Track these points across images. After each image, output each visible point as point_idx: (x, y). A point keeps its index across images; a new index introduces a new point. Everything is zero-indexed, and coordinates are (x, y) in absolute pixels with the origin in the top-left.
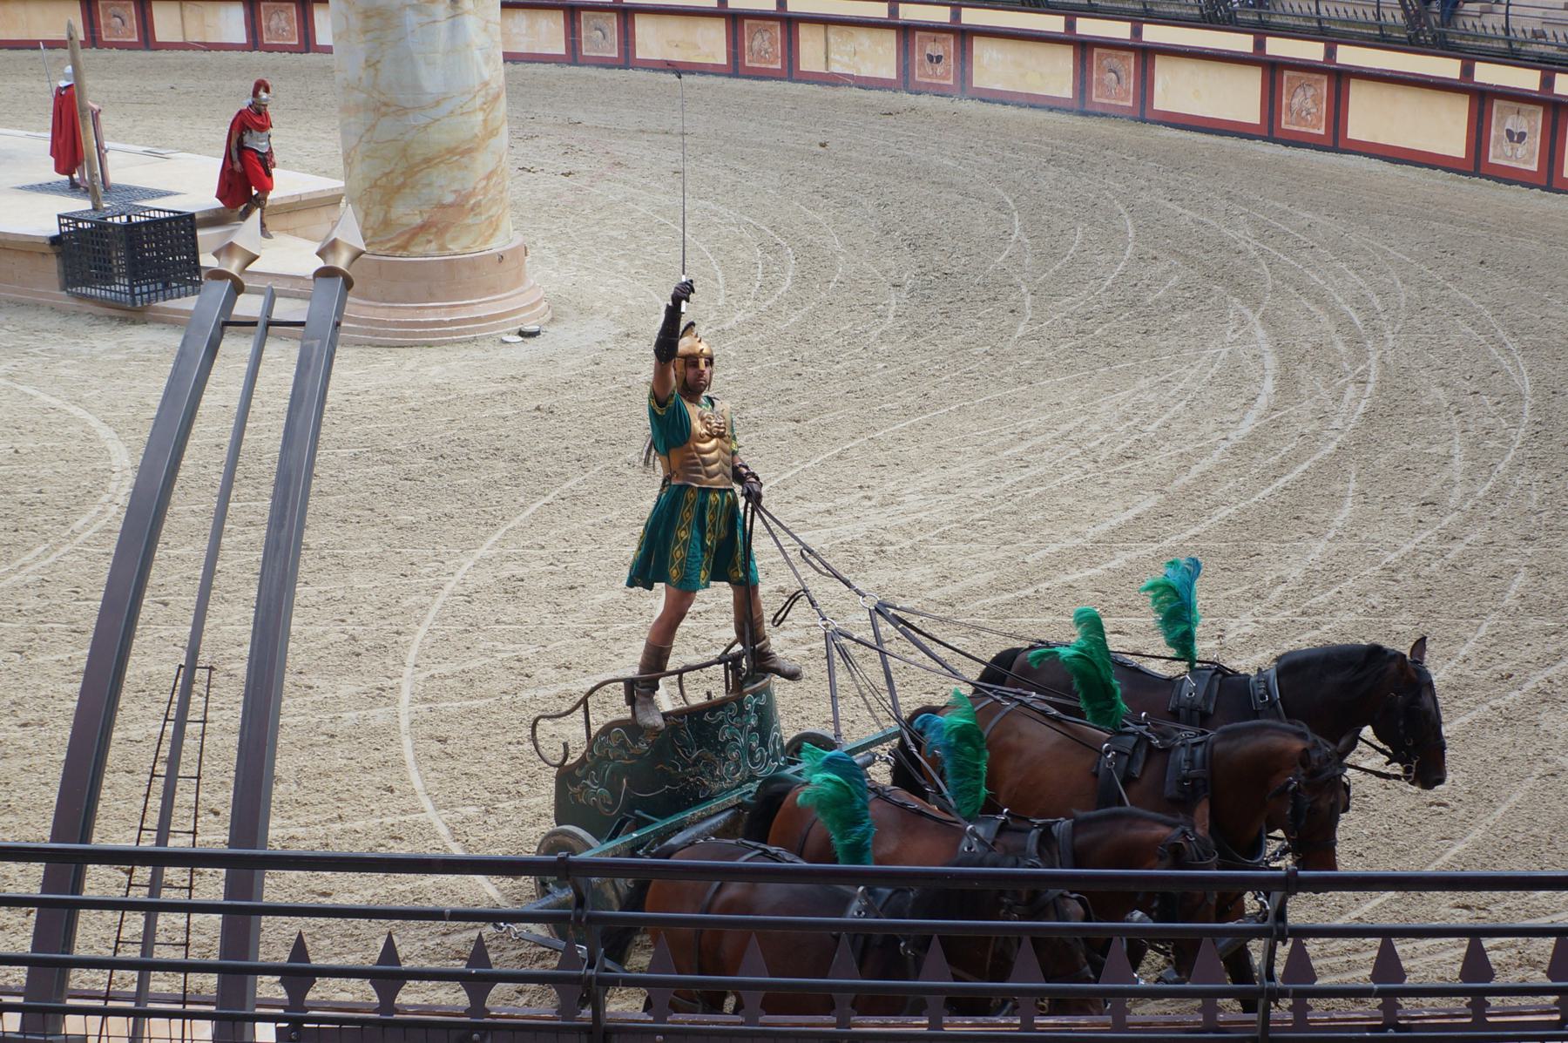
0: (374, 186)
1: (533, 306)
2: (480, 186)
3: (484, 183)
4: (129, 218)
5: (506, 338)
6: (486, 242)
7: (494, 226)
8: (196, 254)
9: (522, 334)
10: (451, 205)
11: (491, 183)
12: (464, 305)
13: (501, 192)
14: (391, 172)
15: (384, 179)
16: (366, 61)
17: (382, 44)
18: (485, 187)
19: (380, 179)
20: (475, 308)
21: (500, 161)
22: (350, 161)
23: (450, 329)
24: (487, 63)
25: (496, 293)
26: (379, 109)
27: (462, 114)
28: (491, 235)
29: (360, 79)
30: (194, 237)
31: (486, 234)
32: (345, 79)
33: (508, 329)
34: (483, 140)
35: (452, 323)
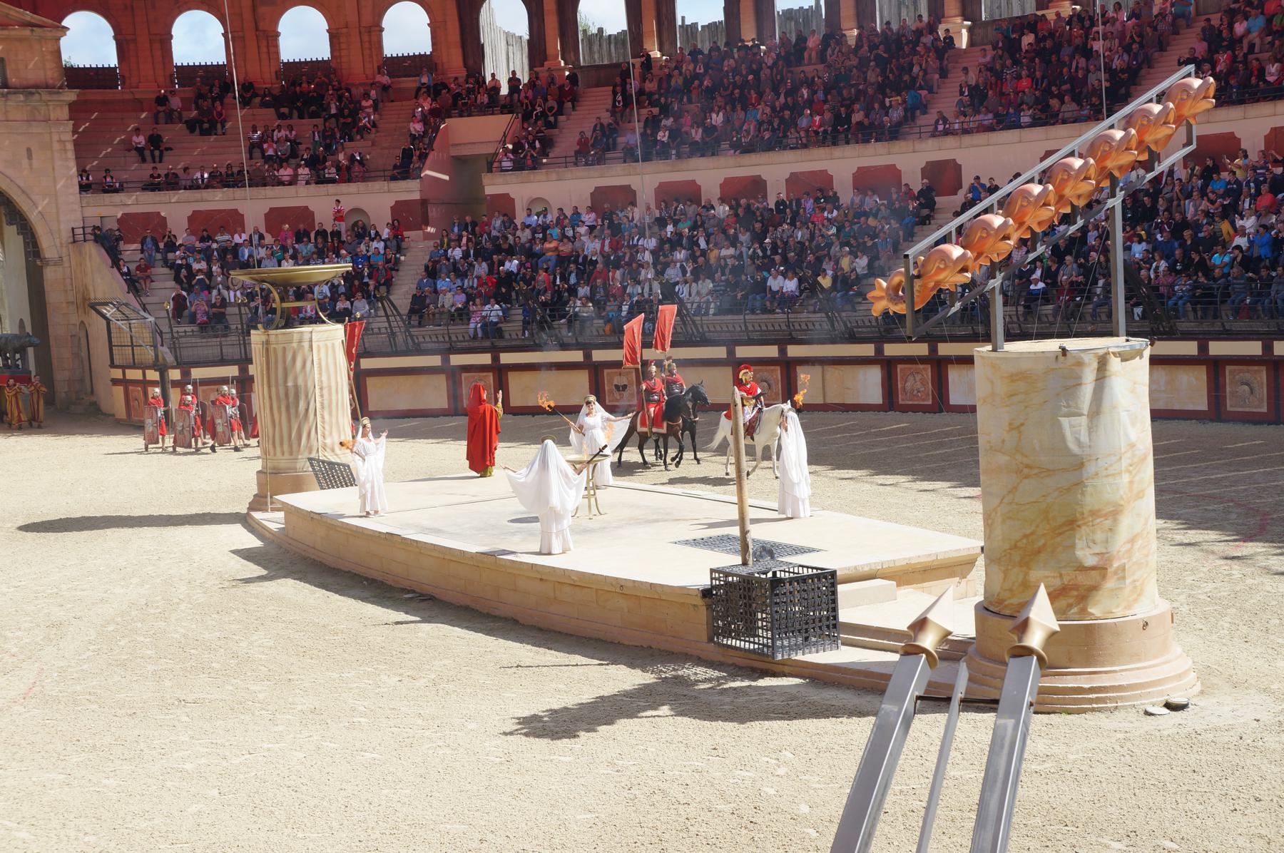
0: (1015, 547)
1: (1179, 677)
2: (1123, 549)
3: (1129, 546)
4: (774, 573)
5: (1151, 710)
6: (1129, 607)
7: (1138, 592)
8: (835, 610)
9: (1170, 706)
10: (1093, 568)
12: (1106, 672)
13: (1147, 556)
14: (1032, 534)
15: (1025, 541)
16: (1010, 424)
17: (1026, 407)
18: (1129, 551)
19: (1020, 540)
20: (1117, 675)
21: (1146, 524)
22: (990, 521)
23: (1090, 696)
24: (1133, 425)
25: (1140, 660)
27: (1107, 476)
28: (1135, 600)
30: (834, 593)
31: (1131, 599)
32: (989, 442)
33: (1154, 700)
34: (1129, 502)
35: (1092, 690)
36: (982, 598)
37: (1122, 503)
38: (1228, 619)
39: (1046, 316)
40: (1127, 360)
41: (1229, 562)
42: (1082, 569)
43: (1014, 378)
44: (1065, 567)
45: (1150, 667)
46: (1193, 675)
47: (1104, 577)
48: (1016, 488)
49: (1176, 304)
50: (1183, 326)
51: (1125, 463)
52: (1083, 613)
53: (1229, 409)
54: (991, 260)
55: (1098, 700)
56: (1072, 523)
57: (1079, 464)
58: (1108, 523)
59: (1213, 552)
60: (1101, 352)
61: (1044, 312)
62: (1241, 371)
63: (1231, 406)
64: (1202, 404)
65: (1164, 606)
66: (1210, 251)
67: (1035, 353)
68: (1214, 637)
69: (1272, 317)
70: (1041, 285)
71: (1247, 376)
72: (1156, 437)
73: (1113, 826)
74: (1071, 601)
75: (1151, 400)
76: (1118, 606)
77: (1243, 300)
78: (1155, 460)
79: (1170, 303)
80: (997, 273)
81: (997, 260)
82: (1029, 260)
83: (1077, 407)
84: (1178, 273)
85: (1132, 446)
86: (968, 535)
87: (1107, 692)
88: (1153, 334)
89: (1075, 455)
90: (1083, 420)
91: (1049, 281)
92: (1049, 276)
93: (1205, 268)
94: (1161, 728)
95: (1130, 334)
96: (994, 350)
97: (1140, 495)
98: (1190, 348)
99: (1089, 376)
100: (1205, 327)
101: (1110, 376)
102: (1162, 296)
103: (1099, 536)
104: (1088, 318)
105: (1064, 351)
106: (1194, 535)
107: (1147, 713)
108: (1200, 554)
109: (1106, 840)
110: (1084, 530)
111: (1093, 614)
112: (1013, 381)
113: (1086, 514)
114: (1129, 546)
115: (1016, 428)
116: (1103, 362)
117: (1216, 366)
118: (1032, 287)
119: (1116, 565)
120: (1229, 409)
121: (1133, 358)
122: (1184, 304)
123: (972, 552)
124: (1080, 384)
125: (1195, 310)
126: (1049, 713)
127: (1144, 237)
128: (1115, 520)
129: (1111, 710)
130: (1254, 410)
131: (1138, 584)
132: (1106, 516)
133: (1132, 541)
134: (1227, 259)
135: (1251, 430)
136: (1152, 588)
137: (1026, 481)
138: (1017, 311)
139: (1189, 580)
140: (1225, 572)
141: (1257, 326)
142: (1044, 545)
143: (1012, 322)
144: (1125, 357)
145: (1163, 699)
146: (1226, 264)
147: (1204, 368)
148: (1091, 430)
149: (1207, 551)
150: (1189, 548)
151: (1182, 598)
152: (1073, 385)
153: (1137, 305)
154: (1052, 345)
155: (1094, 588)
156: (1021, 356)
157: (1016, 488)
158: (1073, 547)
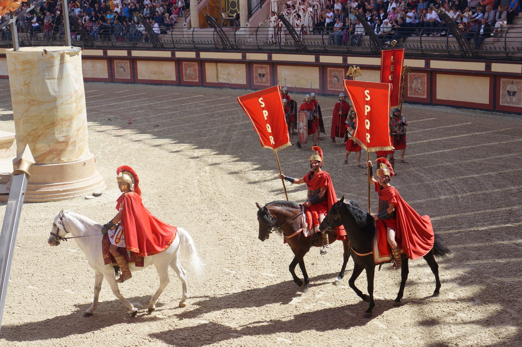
0: (29, 134)
1: (98, 183)
2: (75, 134)
3: (76, 133)
5: (87, 197)
6: (78, 157)
9: (95, 195)
10: (63, 142)
11: (80, 133)
12: (69, 184)
13: (84, 136)
14: (36, 129)
16: (24, 83)
17: (31, 75)
18: (77, 134)
21: (83, 123)
23: (63, 194)
25: (82, 178)
26: (30, 103)
27: (67, 104)
28: (80, 154)
29: (22, 90)
32: (15, 90)
35: (64, 191)
36: (16, 157)
37: (73, 115)
38: (117, 160)
39: (40, 37)
40: (72, 56)
41: (117, 137)
42: (58, 142)
43: (24, 63)
44: (51, 142)
45: (87, 180)
46: (103, 182)
47: (67, 145)
48: (28, 110)
49: (93, 34)
50: (97, 43)
51: (74, 99)
52: (59, 160)
53: (116, 77)
54: (10, 11)
55: (66, 195)
56: (53, 124)
57: (55, 100)
58: (68, 123)
59: (111, 134)
60: (61, 52)
61: (39, 36)
62: (120, 62)
63: (117, 76)
64: (106, 76)
65: (92, 156)
66: (105, 12)
67: (33, 52)
68: (112, 167)
69: (130, 41)
70: (37, 24)
71: (122, 64)
72: (86, 89)
73: (72, 243)
74: (54, 156)
75: (84, 73)
76: (73, 157)
77: (119, 34)
78: (86, 99)
79: (91, 34)
80: (13, 16)
81: (12, 10)
82: (27, 11)
83: (53, 76)
84: (94, 21)
85: (76, 91)
86: (10, 131)
87: (70, 191)
88: (85, 47)
89: (53, 96)
90: (56, 81)
91: (40, 23)
92: (39, 20)
93: (104, 19)
94: (91, 203)
95: (73, 45)
96: (15, 50)
97: (80, 112)
98: (100, 53)
99: (57, 62)
100: (105, 44)
101: (66, 62)
102: (88, 31)
103: (65, 129)
104: (58, 39)
105: (46, 51)
106: (104, 128)
107: (86, 199)
108: (106, 135)
109: (69, 249)
110: (58, 127)
111: (62, 161)
112: (24, 64)
113: (59, 120)
114: (77, 132)
115: (27, 84)
116: (62, 57)
117: (111, 60)
118: (33, 25)
119: (72, 140)
120: (116, 77)
121: (74, 55)
122: (97, 35)
123: (11, 138)
124: (54, 66)
125: (101, 37)
126: (46, 202)
127: (79, 6)
128: (71, 123)
129: (71, 199)
130: (126, 78)
131: (81, 148)
132: (67, 121)
133: (78, 130)
134: (112, 17)
135: (125, 86)
136: (87, 149)
137: (32, 107)
138: (27, 35)
139: (102, 145)
140: (116, 142)
141: (126, 44)
142: (42, 133)
143: (25, 40)
144: (72, 55)
145: (92, 192)
146: (112, 19)
147: (106, 61)
148: (58, 85)
149: (109, 134)
150: (102, 133)
151: (100, 153)
152: (50, 66)
153: (78, 34)
154: (40, 49)
155: (63, 150)
156: (27, 53)
157: (28, 110)
158: (54, 134)
